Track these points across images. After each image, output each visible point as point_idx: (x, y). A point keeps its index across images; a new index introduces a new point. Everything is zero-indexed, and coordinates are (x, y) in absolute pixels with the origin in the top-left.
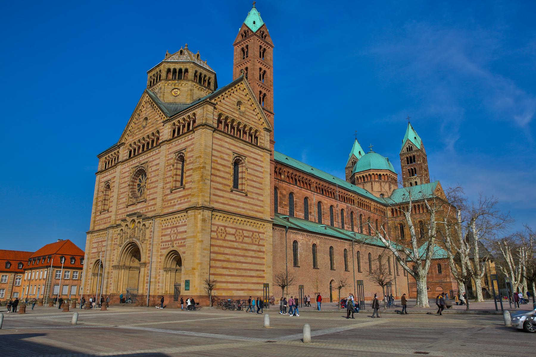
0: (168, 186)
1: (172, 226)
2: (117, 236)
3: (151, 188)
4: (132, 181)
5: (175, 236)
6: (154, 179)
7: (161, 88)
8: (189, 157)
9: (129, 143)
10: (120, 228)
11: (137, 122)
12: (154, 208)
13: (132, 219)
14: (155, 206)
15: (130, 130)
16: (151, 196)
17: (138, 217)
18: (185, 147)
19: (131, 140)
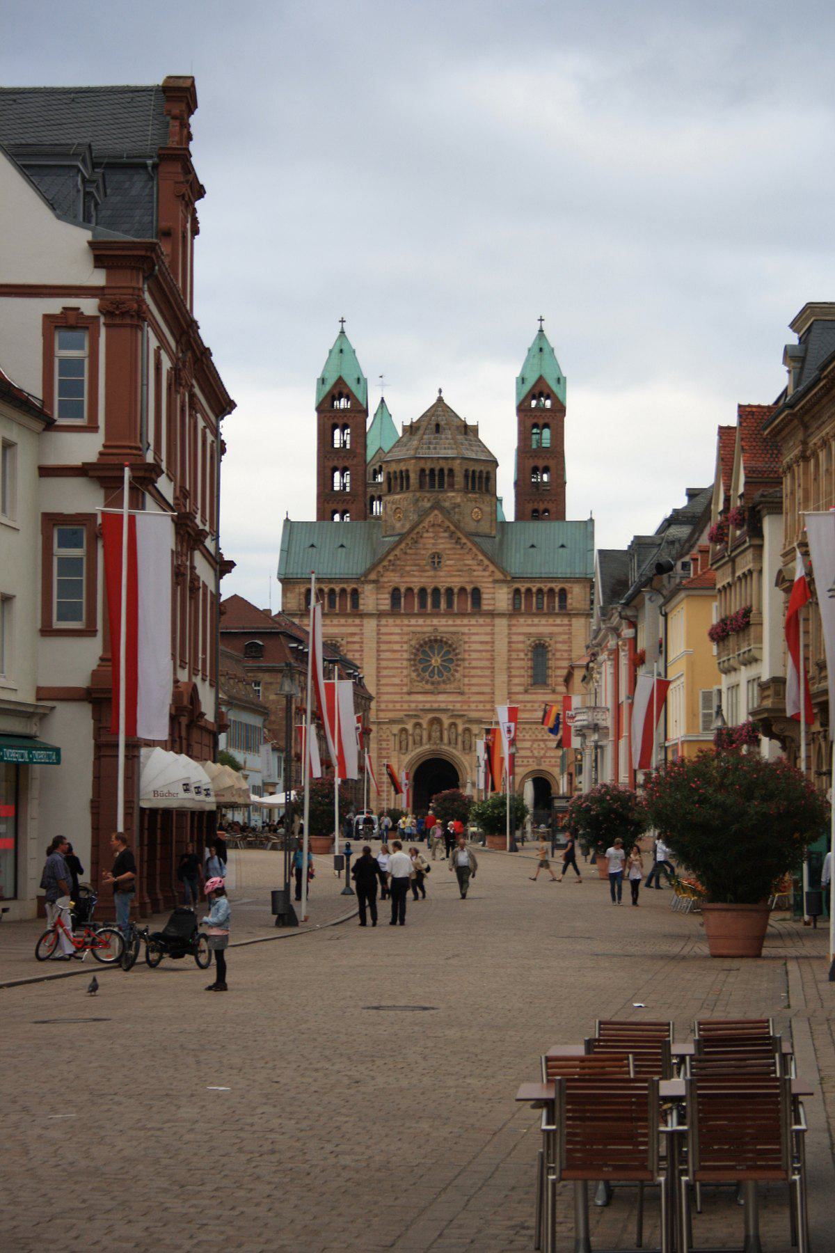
0: (516, 681)
1: (534, 737)
2: (388, 736)
3: (473, 676)
4: (416, 655)
5: (543, 752)
6: (474, 664)
7: (459, 506)
8: (560, 651)
9: (389, 582)
10: (400, 726)
11: (408, 551)
12: (484, 706)
13: (430, 716)
14: (486, 704)
15: (390, 561)
16: (473, 688)
17: (452, 716)
18: (550, 633)
19: (397, 579)
